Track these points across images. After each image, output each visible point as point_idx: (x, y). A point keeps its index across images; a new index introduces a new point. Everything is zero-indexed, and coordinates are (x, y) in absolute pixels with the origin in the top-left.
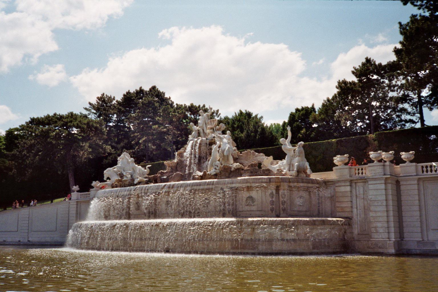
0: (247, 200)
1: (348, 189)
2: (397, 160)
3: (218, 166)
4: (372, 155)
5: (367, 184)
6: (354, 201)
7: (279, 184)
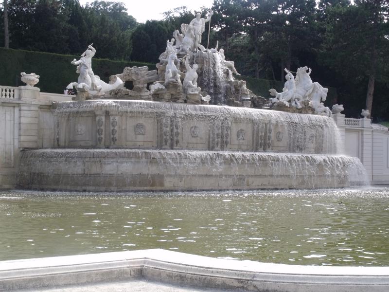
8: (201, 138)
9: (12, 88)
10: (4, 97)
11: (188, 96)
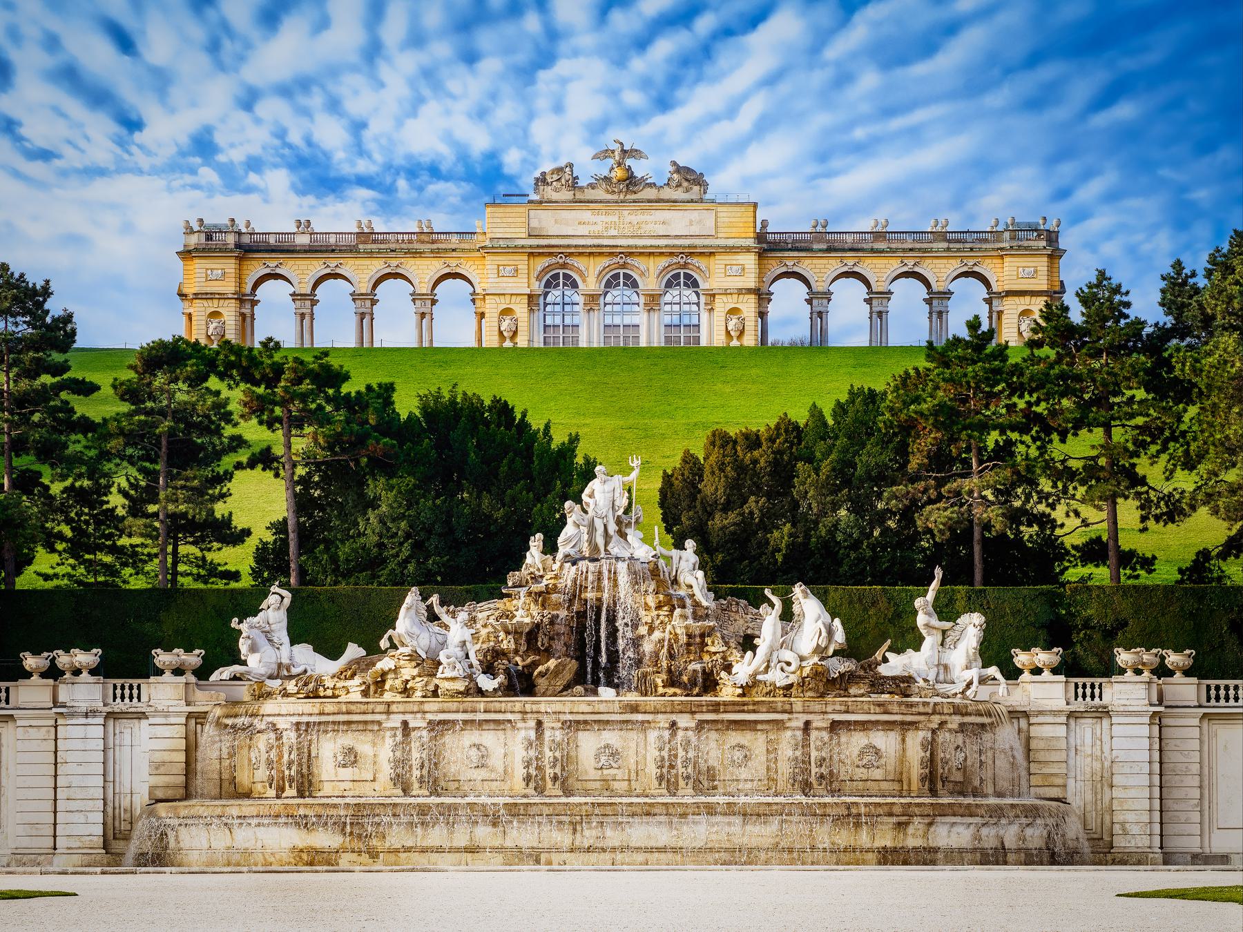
0: (861, 754)
1: (1062, 731)
2: (1162, 671)
5: (1106, 722)
6: (1071, 762)
7: (944, 718)
9: (135, 682)
10: (118, 700)
11: (436, 681)
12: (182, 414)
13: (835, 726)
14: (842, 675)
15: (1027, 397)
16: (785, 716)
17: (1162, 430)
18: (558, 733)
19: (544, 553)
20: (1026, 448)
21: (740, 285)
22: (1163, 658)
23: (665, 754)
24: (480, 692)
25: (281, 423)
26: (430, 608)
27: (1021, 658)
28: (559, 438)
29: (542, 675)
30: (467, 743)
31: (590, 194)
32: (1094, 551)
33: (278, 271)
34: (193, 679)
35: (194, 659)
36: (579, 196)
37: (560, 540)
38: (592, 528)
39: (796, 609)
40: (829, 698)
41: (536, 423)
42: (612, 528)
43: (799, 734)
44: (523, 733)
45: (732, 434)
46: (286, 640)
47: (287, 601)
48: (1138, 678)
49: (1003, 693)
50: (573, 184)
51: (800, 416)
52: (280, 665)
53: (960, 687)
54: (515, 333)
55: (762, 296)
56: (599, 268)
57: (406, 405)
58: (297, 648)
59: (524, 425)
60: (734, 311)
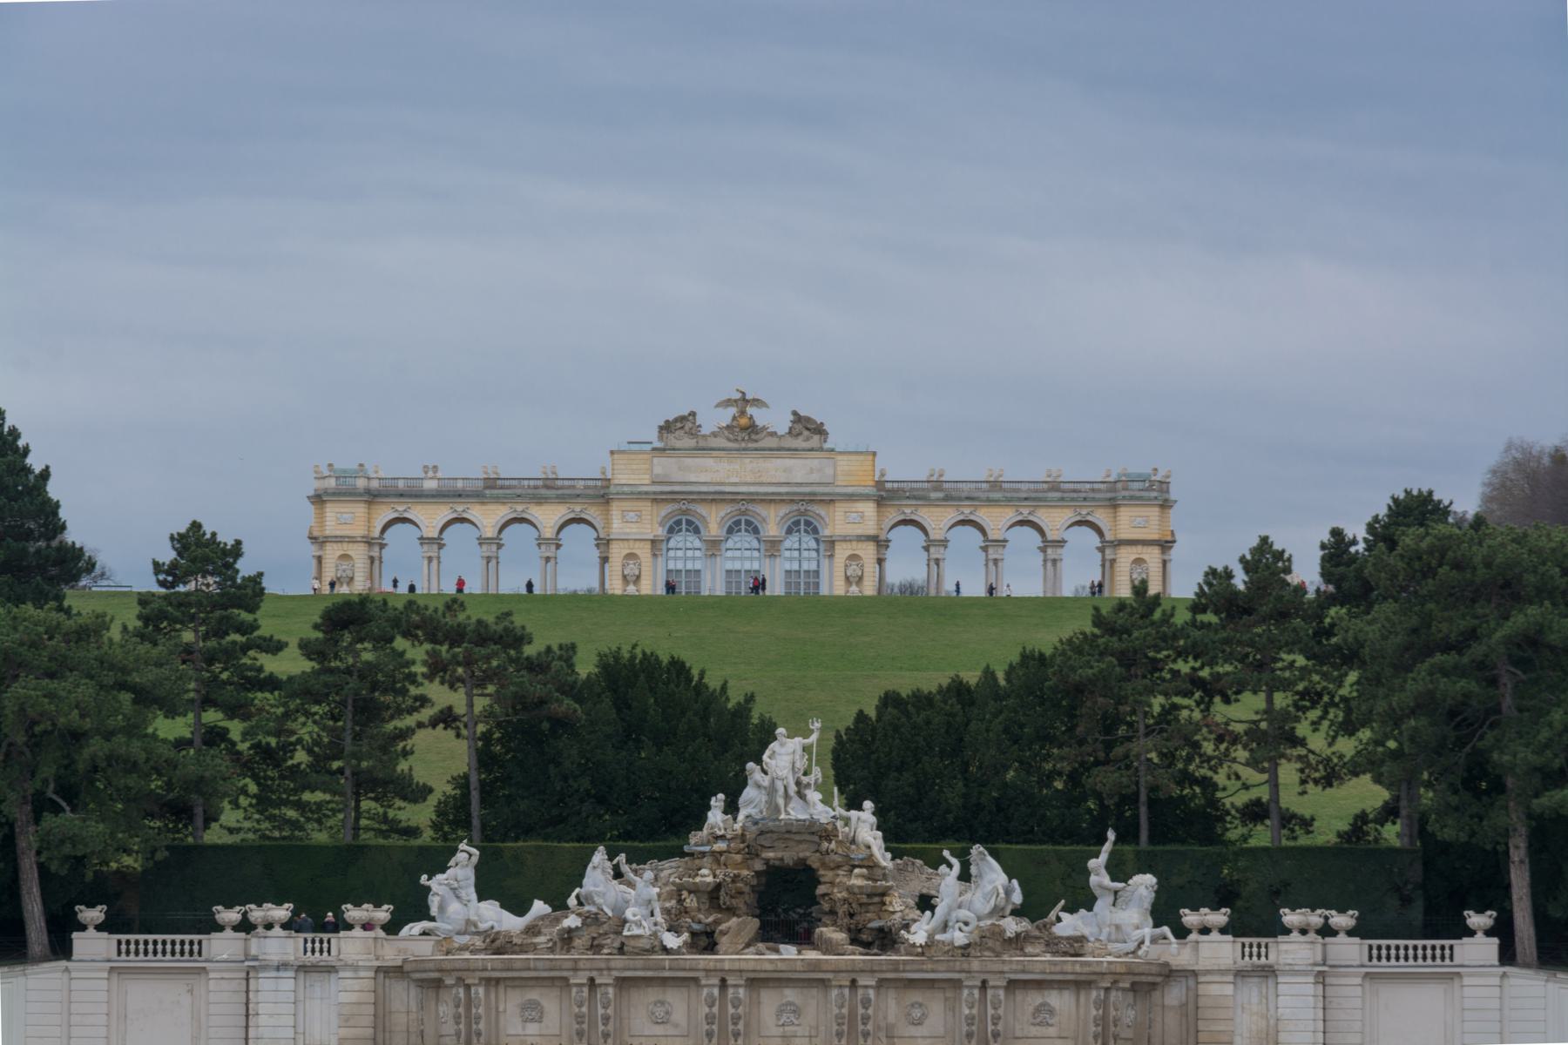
0: (1038, 1010)
1: (1229, 990)
2: (1327, 931)
3: (966, 924)
4: (1290, 918)
5: (1271, 982)
8: (676, 1026)
12: (366, 673)
13: (1013, 985)
14: (1018, 935)
15: (1192, 663)
16: (962, 976)
17: (1320, 695)
18: (741, 991)
19: (725, 812)
20: (1189, 710)
21: (859, 532)
22: (1326, 918)
23: (845, 1011)
24: (665, 950)
25: (463, 681)
26: (616, 869)
27: (1190, 918)
28: (735, 698)
29: (723, 933)
30: (652, 999)
31: (714, 442)
32: (1255, 812)
33: (406, 515)
34: (382, 934)
35: (383, 914)
36: (702, 444)
37: (741, 800)
38: (771, 791)
39: (973, 870)
40: (1006, 957)
41: (713, 682)
42: (793, 789)
43: (976, 992)
44: (705, 991)
45: (904, 695)
46: (474, 896)
47: (475, 859)
48: (1303, 938)
49: (1176, 953)
50: (694, 432)
51: (972, 677)
52: (468, 922)
53: (1131, 946)
54: (638, 577)
55: (881, 543)
56: (722, 514)
57: (585, 668)
58: (484, 904)
59: (700, 688)
60: (854, 557)
